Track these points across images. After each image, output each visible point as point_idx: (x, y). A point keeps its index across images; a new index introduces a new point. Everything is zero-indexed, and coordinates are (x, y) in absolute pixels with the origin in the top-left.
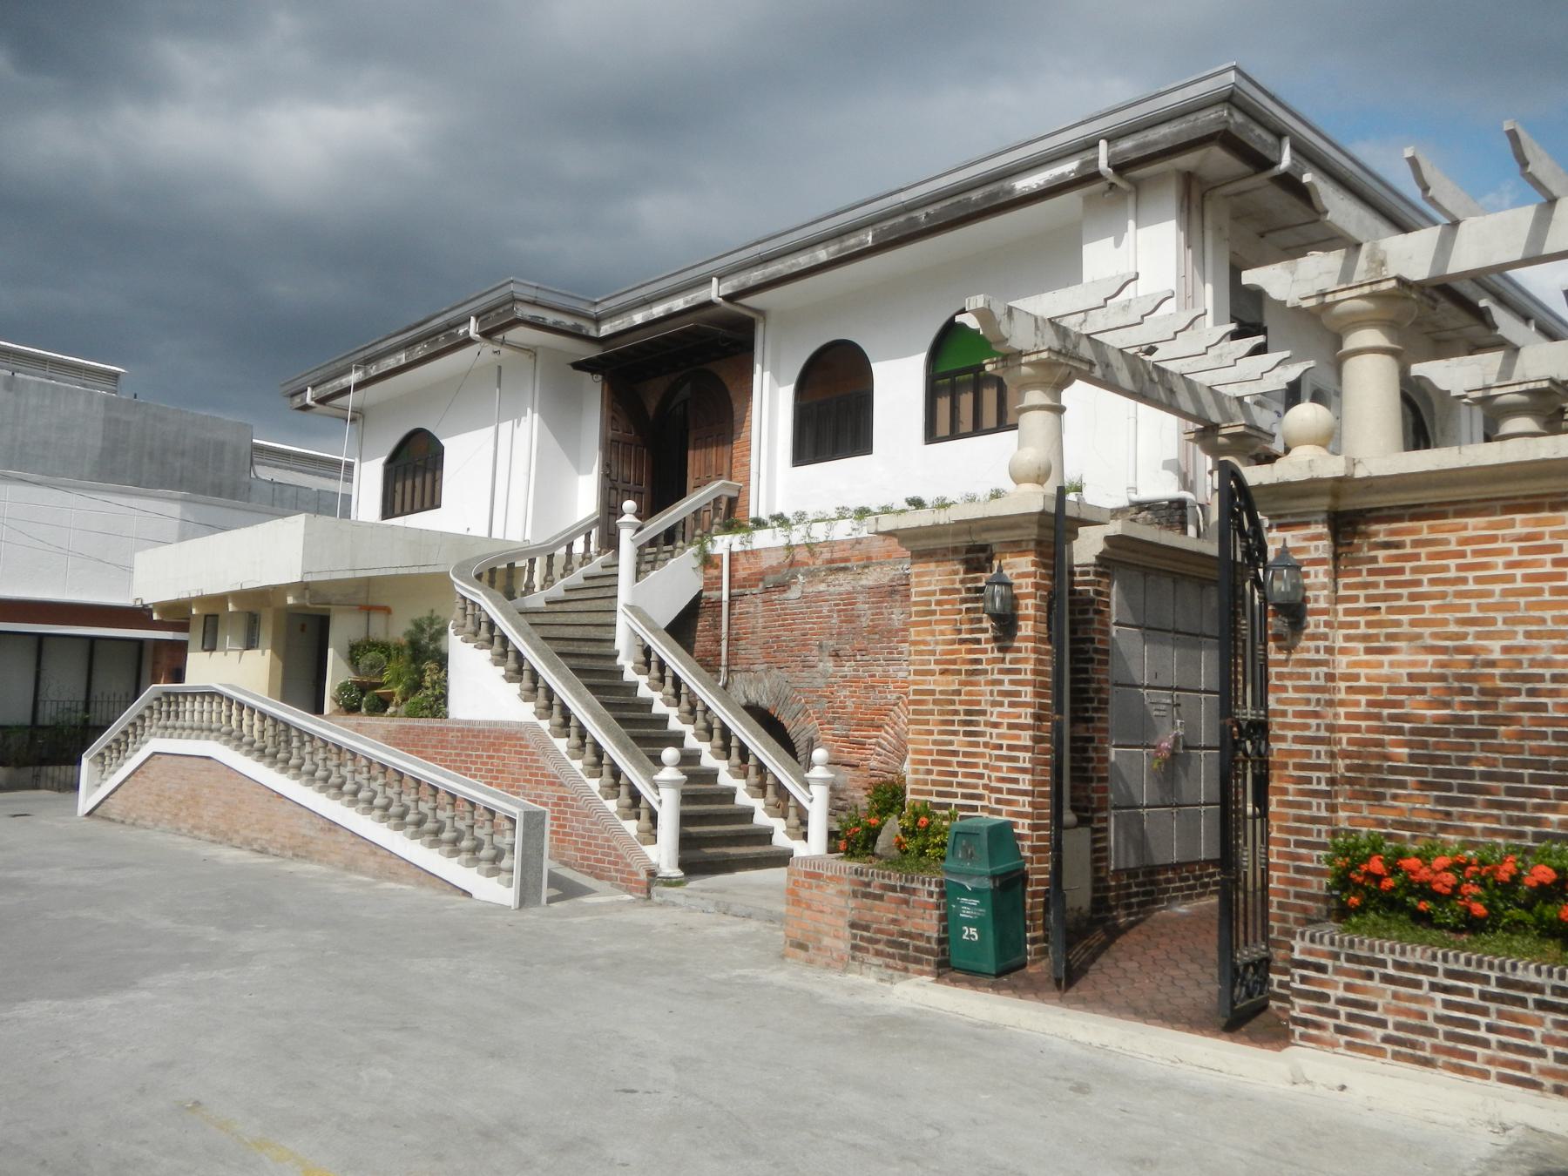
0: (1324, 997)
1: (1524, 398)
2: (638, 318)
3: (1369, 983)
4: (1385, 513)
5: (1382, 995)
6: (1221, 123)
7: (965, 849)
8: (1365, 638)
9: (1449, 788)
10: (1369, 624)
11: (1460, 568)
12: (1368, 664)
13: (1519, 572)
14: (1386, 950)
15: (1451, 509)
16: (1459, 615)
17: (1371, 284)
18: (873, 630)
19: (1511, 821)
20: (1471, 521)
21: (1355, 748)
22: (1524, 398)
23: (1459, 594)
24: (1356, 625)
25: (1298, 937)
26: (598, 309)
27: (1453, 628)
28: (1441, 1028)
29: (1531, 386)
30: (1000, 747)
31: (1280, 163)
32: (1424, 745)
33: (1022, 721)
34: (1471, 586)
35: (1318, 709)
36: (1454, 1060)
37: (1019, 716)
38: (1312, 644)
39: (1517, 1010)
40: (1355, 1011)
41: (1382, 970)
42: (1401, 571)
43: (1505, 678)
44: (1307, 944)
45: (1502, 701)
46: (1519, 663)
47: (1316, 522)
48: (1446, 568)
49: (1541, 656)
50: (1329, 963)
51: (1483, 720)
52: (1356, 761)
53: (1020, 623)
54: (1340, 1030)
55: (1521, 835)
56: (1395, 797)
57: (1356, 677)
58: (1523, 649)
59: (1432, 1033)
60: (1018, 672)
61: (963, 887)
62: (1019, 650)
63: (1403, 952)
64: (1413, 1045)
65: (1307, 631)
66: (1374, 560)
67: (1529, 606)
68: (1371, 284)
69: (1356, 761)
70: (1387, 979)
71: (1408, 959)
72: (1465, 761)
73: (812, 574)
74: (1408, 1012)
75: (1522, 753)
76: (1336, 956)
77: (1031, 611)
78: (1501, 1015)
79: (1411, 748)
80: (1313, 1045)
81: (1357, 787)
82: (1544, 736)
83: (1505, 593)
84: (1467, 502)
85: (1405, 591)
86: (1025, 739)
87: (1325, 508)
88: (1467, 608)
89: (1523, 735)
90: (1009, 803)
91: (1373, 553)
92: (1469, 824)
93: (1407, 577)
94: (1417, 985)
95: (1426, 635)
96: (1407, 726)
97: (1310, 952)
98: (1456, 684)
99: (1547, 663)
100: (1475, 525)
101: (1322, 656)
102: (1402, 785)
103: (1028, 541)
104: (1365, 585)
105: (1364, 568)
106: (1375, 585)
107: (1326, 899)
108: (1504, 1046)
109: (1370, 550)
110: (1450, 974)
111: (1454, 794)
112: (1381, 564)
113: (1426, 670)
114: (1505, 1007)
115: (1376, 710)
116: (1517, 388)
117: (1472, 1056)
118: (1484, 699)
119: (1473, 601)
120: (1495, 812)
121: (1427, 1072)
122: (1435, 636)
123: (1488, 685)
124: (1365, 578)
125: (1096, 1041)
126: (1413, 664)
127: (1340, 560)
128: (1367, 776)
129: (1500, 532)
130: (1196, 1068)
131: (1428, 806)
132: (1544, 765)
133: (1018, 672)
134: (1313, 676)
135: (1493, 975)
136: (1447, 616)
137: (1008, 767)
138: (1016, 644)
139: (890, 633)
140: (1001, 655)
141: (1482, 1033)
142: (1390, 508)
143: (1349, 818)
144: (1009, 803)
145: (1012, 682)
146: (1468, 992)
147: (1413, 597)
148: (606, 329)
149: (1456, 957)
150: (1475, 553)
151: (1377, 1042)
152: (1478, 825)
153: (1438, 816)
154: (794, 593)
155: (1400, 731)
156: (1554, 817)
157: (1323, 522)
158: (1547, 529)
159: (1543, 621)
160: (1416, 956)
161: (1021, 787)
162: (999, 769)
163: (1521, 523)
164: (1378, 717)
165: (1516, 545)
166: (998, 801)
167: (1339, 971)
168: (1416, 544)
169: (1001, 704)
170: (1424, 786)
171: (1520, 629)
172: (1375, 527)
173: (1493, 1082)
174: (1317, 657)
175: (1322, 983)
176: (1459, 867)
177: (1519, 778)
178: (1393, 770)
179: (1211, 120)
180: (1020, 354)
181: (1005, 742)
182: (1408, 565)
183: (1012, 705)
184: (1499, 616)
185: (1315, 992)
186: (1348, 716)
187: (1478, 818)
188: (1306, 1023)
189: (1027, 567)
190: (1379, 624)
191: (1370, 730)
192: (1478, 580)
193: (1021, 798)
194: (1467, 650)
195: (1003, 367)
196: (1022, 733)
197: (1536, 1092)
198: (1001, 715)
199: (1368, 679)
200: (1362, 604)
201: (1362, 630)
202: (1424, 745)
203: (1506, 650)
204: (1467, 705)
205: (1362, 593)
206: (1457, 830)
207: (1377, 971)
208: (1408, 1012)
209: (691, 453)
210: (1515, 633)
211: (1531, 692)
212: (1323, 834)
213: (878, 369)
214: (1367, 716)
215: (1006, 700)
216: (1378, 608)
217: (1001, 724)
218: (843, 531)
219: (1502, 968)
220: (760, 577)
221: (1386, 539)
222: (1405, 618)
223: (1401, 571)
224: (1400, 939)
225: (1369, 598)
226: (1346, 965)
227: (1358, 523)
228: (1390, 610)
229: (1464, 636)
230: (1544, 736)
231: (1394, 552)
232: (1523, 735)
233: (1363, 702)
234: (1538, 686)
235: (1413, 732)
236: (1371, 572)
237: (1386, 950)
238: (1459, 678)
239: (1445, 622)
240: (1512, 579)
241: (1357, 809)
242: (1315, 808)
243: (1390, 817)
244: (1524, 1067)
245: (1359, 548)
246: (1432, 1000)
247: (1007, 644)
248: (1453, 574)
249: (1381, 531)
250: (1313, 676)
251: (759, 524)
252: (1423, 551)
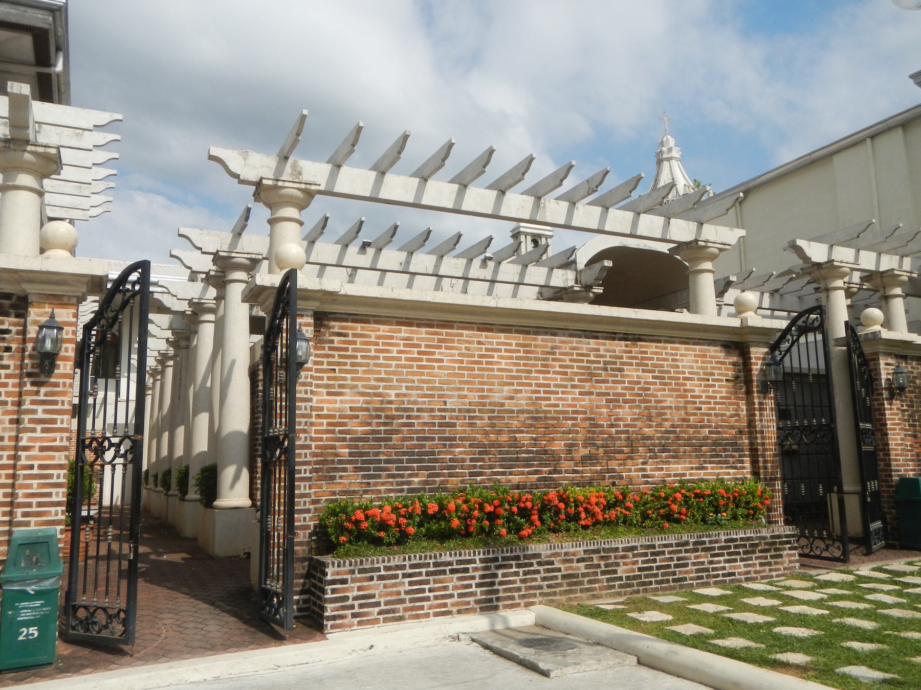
0: (346, 598)
1: (248, 262)
3: (371, 583)
4: (338, 316)
5: (377, 588)
6: (47, 24)
7: (29, 558)
8: (327, 386)
9: (368, 469)
10: (329, 378)
11: (376, 351)
12: (328, 402)
13: (403, 356)
14: (380, 561)
15: (372, 319)
16: (375, 376)
17: (306, 183)
19: (398, 484)
20: (382, 327)
21: (319, 451)
22: (248, 262)
23: (376, 365)
24: (321, 378)
25: (330, 566)
27: (373, 383)
28: (408, 597)
29: (253, 256)
30: (31, 467)
31: (55, 66)
32: (357, 447)
33: (57, 443)
34: (381, 361)
35: (306, 428)
36: (414, 613)
37: (55, 440)
38: (303, 388)
39: (442, 577)
40: (363, 601)
41: (378, 574)
42: (346, 349)
43: (397, 410)
44: (336, 569)
45: (395, 422)
46: (403, 402)
47: (307, 316)
48: (369, 351)
49: (412, 399)
50: (349, 577)
51: (386, 432)
52: (320, 458)
53: (58, 363)
54: (354, 615)
55: (402, 491)
56: (341, 477)
57: (322, 409)
58: (405, 395)
59: (402, 601)
60: (55, 403)
61: (25, 592)
62: (56, 385)
63: (389, 561)
64: (394, 611)
65: (300, 381)
66: (332, 342)
67: (408, 373)
68: (306, 183)
69: (320, 458)
70: (381, 578)
71: (392, 564)
72: (377, 454)
74: (391, 594)
75: (403, 448)
76: (353, 572)
77: (71, 354)
78: (435, 582)
79: (350, 449)
80: (338, 630)
81: (320, 474)
82: (412, 439)
83: (397, 366)
84: (380, 316)
85: (348, 361)
86: (60, 459)
87: (314, 308)
88: (379, 372)
89: (404, 439)
90: (39, 514)
91: (332, 338)
92: (378, 488)
93: (350, 353)
94: (396, 577)
95: (359, 386)
96: (348, 436)
97: (338, 573)
98: (374, 413)
99: (415, 403)
100: (383, 329)
101: (309, 396)
102: (345, 470)
103: (70, 297)
104: (327, 356)
105: (327, 346)
106: (333, 356)
107: (308, 543)
108: (436, 598)
109: (330, 336)
110: (412, 566)
111: (372, 472)
112: (336, 345)
113: (359, 405)
114: (437, 577)
115: (332, 428)
116: (246, 256)
117: (422, 608)
118: (387, 421)
119: (382, 369)
120: (391, 480)
121: (401, 624)
122: (364, 386)
123: (389, 413)
124: (327, 352)
125: (209, 676)
126: (353, 402)
128: (326, 466)
129: (395, 335)
130: (292, 667)
131: (358, 481)
132: (413, 454)
133: (55, 403)
134: (303, 408)
135: (431, 561)
136: (370, 376)
137: (38, 484)
138: (52, 380)
140: (35, 389)
141: (427, 594)
142: (362, 315)
143: (315, 493)
144: (39, 514)
145: (46, 412)
146: (420, 574)
147: (353, 365)
149: (415, 556)
150: (384, 344)
151: (376, 616)
152: (383, 488)
153: (363, 485)
155: (344, 440)
156: (416, 480)
157: (311, 316)
158: (415, 336)
159: (413, 381)
160: (396, 561)
161: (54, 499)
162: (29, 486)
163: (404, 331)
164: (333, 432)
165: (402, 342)
166: (25, 515)
167: (353, 581)
168: (354, 335)
169: (33, 430)
170: (357, 469)
171: (404, 385)
172: (332, 323)
173: (431, 618)
174: (306, 396)
175: (344, 590)
176: (395, 509)
177: (401, 461)
178: (340, 462)
179: (39, 18)
180: (27, 142)
181: (36, 463)
182: (351, 347)
183: (44, 430)
184: (395, 378)
185: (340, 597)
186: (316, 432)
187: (383, 484)
188: (334, 618)
189: (68, 317)
190: (335, 379)
191: (328, 439)
192: (385, 358)
193: (53, 509)
194: (379, 395)
195: (5, 147)
196: (57, 454)
197: (450, 616)
198: (31, 439)
199: (328, 410)
200: (325, 367)
201: (325, 382)
202: (357, 447)
203: (397, 395)
204: (378, 424)
205: (325, 360)
206: (372, 492)
207: (375, 574)
208: (391, 594)
210: (402, 386)
211: (408, 417)
212: (307, 504)
214: (328, 432)
215: (39, 427)
216: (334, 370)
217: (33, 447)
219: (435, 558)
221: (339, 331)
222: (349, 376)
223: (346, 349)
224: (373, 555)
225: (329, 363)
226: (358, 576)
227: (323, 319)
228: (341, 371)
229: (378, 387)
230: (412, 439)
231: (343, 338)
232: (404, 439)
233: (325, 423)
234: (411, 414)
235: (351, 440)
236: (330, 349)
237: (380, 561)
238: (376, 409)
239: (369, 379)
240: (400, 359)
241: (320, 487)
242: (302, 489)
243: (338, 489)
244: (445, 605)
245: (324, 334)
246: (404, 583)
247: (42, 379)
248: (373, 354)
249: (336, 326)
250: (303, 408)
252: (358, 340)
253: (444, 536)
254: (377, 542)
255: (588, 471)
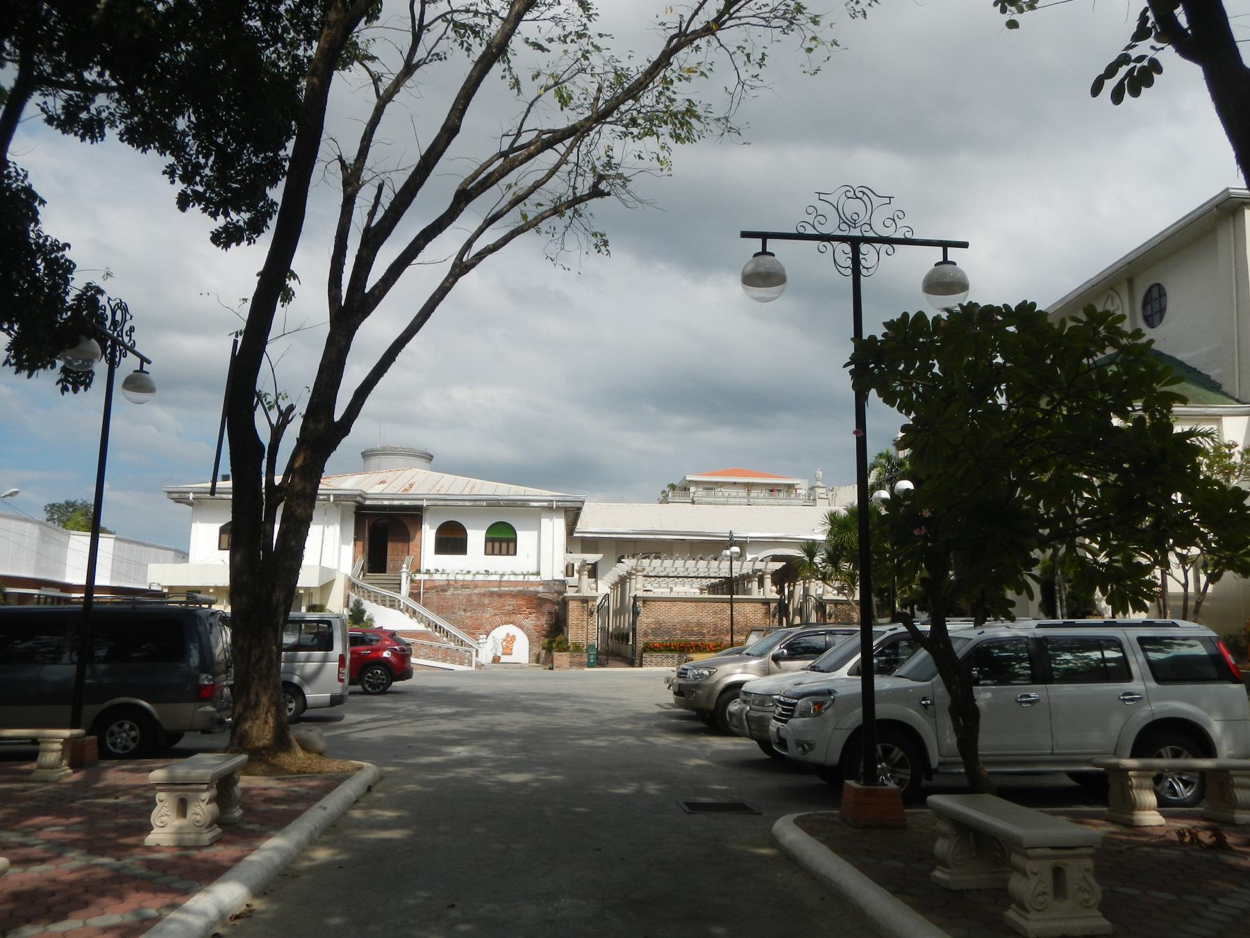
2: (386, 503)
5: (653, 659)
18: (478, 604)
26: (368, 496)
73: (456, 588)
100: (659, 603)
127: (644, 606)
139: (484, 605)
148: (368, 502)
154: (449, 593)
209: (389, 544)
213: (469, 531)
218: (469, 577)
220: (436, 587)
251: (428, 572)
253: (671, 651)
254: (655, 651)
255: (713, 638)
